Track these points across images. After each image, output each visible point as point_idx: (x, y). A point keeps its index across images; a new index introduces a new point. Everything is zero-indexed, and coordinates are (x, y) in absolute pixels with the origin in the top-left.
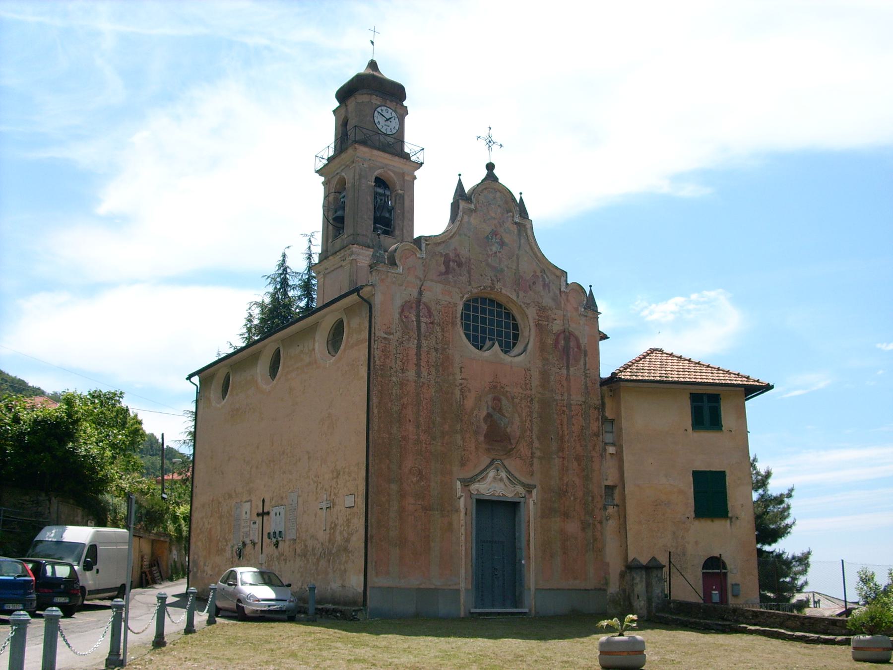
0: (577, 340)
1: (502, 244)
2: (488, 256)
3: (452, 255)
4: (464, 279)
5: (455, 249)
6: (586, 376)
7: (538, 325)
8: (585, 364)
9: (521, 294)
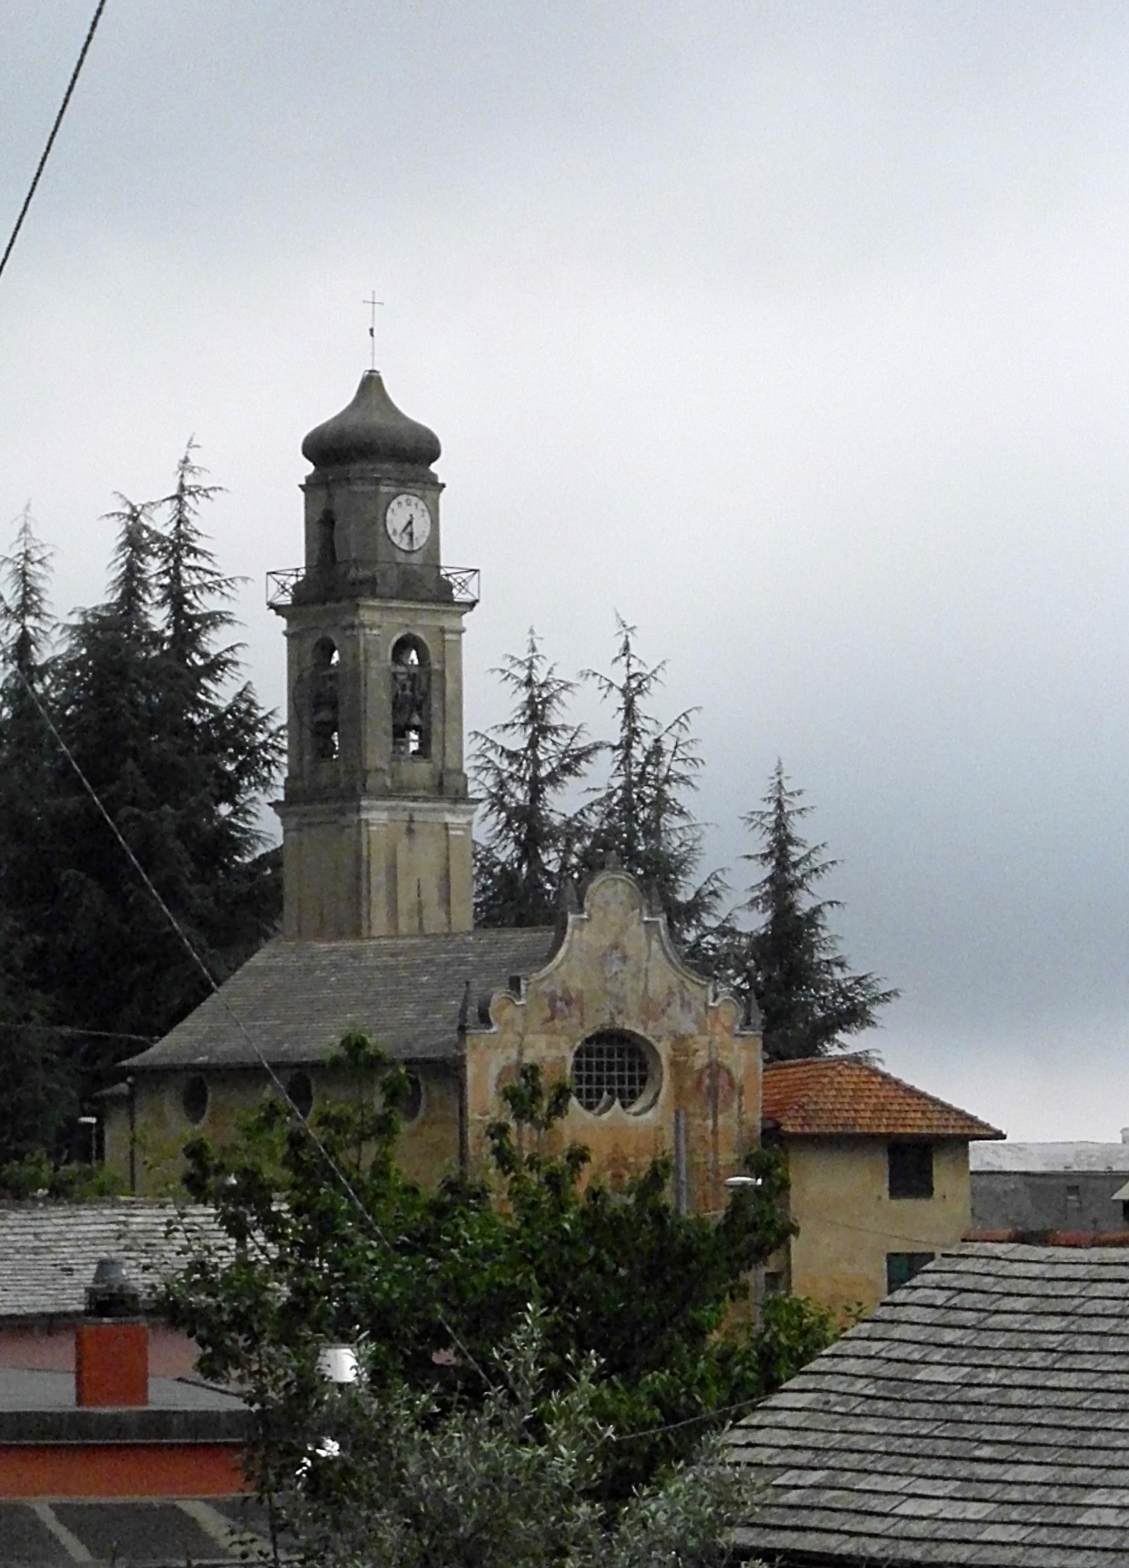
0: (729, 1072)
1: (624, 959)
2: (606, 980)
3: (559, 993)
4: (575, 1020)
5: (564, 982)
6: (741, 1123)
7: (674, 1064)
8: (740, 1107)
9: (651, 1025)
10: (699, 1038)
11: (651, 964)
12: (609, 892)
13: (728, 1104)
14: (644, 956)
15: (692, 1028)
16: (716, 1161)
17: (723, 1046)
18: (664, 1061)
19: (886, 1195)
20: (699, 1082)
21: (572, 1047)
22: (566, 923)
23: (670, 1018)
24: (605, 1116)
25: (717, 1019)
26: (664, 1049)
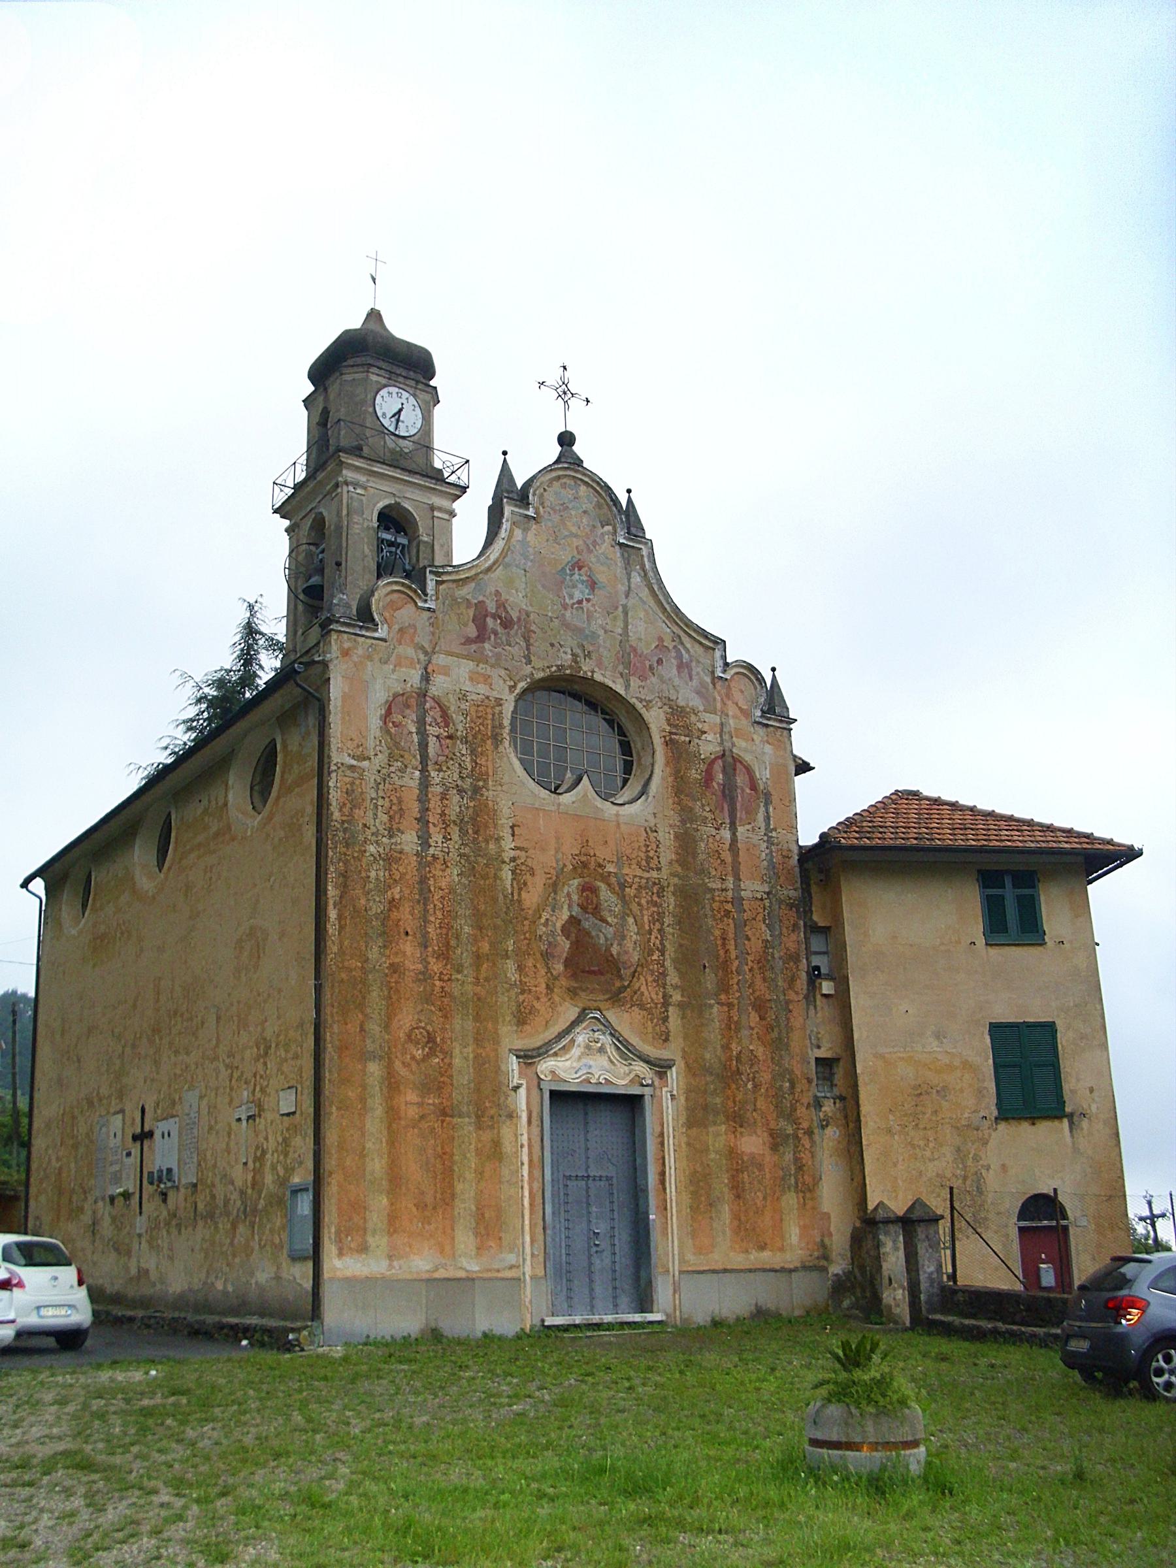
0: (749, 770)
1: (593, 585)
2: (565, 606)
3: (491, 607)
4: (517, 651)
5: (497, 593)
6: (770, 842)
7: (669, 743)
8: (767, 818)
9: (634, 682)
10: (707, 717)
11: (631, 602)
12: (568, 494)
13: (751, 812)
14: (622, 588)
15: (696, 702)
16: (737, 889)
17: (739, 733)
18: (658, 741)
19: (981, 941)
20: (709, 777)
21: (512, 688)
22: (502, 514)
23: (661, 678)
24: (566, 798)
25: (728, 695)
26: (656, 719)
